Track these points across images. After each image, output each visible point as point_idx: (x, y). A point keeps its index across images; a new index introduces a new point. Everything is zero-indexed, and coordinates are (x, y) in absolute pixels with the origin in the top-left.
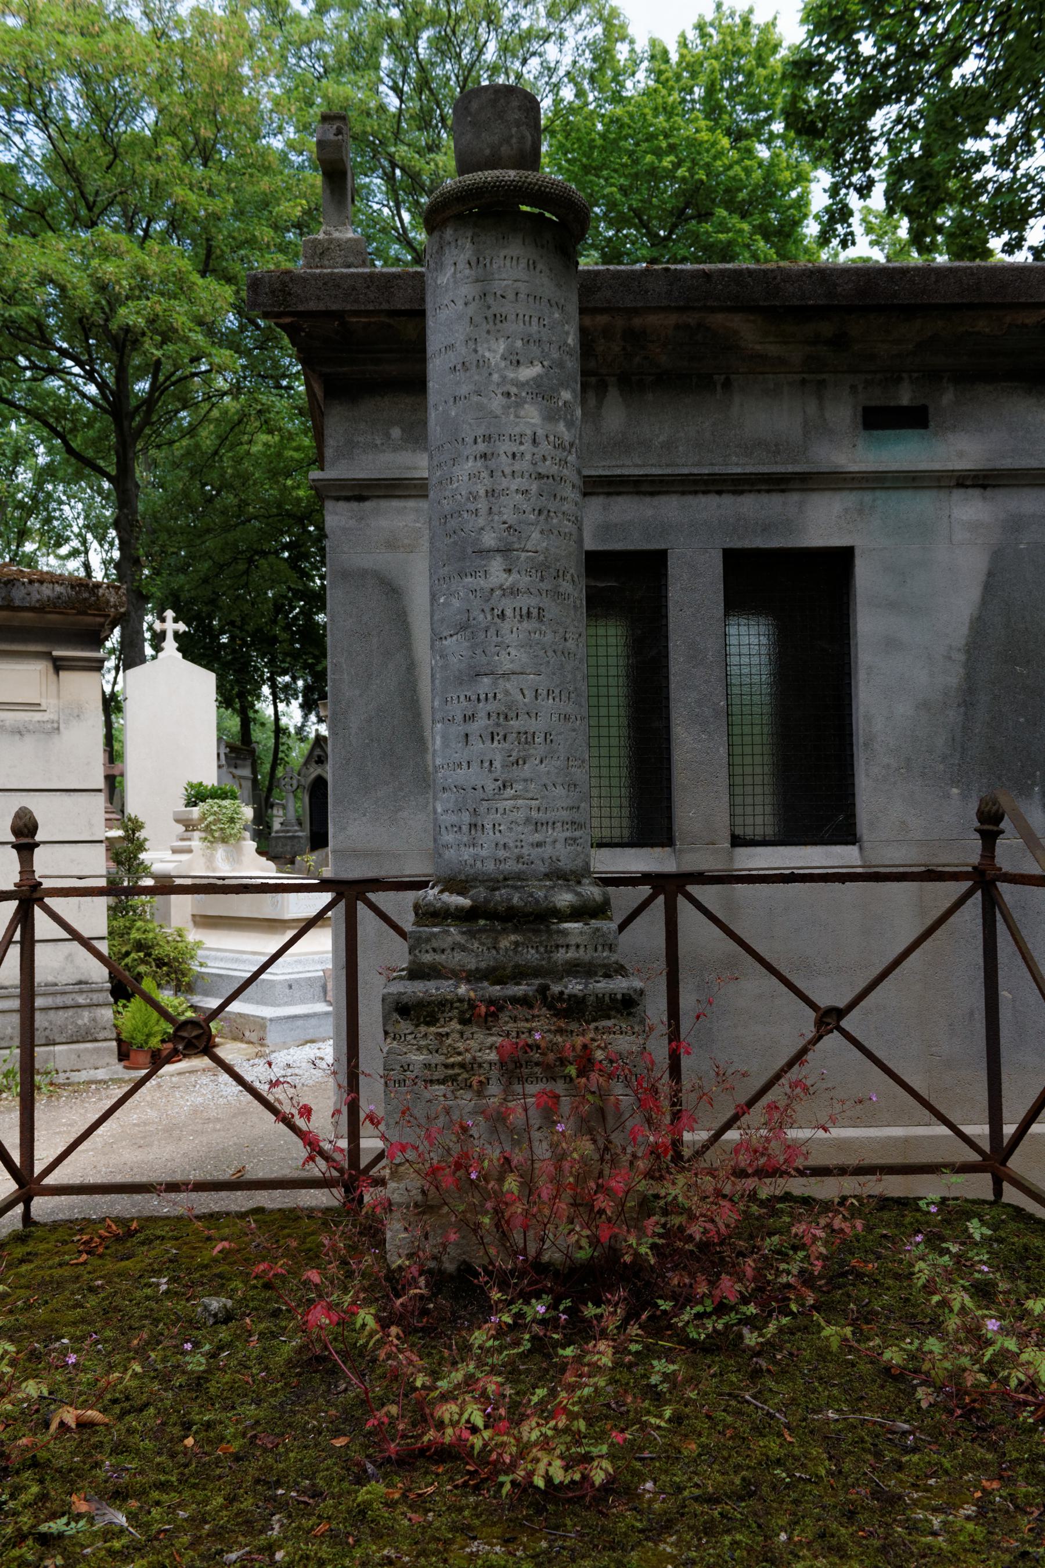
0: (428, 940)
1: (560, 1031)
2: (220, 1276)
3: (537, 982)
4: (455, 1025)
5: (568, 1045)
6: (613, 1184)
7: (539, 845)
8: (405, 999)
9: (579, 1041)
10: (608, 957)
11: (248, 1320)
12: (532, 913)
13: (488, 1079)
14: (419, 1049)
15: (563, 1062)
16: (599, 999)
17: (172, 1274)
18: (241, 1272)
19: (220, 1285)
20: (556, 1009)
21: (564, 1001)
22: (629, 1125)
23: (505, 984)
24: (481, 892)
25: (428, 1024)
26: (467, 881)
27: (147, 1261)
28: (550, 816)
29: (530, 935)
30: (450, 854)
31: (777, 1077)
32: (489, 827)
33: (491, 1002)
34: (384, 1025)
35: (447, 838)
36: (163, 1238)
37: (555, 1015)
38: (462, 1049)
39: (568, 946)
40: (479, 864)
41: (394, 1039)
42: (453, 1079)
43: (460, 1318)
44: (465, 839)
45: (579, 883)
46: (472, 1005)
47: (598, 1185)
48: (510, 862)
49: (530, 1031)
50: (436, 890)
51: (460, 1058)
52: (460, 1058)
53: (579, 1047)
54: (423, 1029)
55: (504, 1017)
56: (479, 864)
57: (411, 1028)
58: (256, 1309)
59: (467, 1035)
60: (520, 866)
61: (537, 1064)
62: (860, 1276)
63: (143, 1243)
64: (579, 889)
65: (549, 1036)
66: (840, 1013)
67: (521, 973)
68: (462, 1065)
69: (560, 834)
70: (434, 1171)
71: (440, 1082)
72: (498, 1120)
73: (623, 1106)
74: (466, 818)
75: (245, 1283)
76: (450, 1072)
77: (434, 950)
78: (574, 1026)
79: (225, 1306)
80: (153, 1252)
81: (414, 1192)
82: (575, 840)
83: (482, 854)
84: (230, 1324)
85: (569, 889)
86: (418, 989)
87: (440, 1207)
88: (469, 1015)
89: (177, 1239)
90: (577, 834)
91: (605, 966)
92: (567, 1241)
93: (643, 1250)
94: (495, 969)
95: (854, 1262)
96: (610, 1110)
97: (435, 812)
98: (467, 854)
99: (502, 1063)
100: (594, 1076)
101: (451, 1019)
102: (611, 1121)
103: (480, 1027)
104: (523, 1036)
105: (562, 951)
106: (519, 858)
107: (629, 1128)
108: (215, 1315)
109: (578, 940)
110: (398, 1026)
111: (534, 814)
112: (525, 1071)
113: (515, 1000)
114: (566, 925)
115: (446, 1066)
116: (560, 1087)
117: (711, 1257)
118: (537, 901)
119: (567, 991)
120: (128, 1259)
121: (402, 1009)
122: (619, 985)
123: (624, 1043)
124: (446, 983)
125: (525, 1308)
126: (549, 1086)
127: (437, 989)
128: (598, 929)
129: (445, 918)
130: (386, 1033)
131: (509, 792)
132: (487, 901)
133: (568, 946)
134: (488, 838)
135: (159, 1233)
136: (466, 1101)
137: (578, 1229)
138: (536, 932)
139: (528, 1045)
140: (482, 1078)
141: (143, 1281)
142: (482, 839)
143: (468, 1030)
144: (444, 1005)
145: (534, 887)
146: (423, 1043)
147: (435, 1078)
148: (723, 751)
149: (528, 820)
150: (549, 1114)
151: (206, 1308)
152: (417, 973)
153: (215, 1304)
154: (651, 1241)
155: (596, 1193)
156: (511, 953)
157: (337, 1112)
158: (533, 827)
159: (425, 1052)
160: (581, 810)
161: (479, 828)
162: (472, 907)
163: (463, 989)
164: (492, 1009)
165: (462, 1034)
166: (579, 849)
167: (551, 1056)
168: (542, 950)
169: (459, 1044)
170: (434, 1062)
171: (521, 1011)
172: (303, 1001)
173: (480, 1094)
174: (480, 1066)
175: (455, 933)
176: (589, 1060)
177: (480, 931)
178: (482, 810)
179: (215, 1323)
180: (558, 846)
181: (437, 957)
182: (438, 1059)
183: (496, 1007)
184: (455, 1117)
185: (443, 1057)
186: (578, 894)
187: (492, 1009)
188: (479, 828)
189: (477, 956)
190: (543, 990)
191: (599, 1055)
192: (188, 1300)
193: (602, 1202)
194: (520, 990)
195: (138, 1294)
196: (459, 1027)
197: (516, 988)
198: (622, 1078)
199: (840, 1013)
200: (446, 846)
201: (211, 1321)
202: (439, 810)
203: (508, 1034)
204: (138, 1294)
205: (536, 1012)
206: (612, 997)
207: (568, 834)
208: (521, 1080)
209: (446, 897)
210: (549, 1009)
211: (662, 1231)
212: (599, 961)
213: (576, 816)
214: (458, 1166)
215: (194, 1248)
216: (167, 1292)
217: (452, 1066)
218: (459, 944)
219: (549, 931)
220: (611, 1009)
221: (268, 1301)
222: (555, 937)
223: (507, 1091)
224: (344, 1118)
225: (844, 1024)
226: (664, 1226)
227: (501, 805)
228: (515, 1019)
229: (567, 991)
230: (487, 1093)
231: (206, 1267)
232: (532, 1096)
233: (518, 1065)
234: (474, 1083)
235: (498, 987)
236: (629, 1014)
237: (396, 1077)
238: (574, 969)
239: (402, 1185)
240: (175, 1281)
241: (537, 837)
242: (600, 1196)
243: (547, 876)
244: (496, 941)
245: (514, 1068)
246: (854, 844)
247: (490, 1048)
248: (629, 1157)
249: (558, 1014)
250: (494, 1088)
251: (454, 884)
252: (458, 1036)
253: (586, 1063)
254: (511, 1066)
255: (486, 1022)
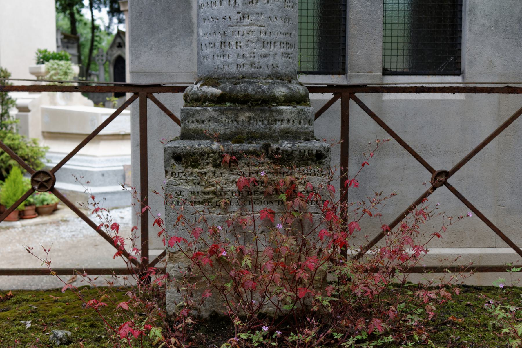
0: (194, 115)
1: (277, 172)
2: (64, 320)
3: (262, 142)
4: (210, 168)
5: (281, 181)
6: (308, 263)
7: (265, 56)
8: (179, 151)
9: (288, 179)
10: (308, 128)
11: (81, 343)
12: (260, 99)
13: (231, 202)
14: (187, 182)
15: (277, 191)
16: (302, 153)
17: (34, 319)
18: (76, 319)
19: (64, 324)
20: (274, 159)
21: (280, 154)
22: (318, 231)
23: (242, 143)
24: (228, 86)
25: (193, 167)
26: (218, 79)
27: (18, 312)
28: (273, 38)
29: (258, 113)
30: (208, 62)
31: (410, 209)
32: (233, 43)
33: (233, 154)
34: (165, 167)
35: (206, 51)
36: (28, 300)
37: (273, 163)
38: (214, 183)
39: (282, 120)
40: (226, 68)
41: (172, 175)
42: (209, 201)
43: (211, 343)
44: (218, 52)
45: (290, 82)
46: (221, 155)
47: (298, 265)
48: (246, 67)
49: (258, 172)
50: (199, 85)
51: (213, 188)
52: (213, 188)
53: (288, 182)
54: (190, 170)
55: (241, 163)
56: (226, 68)
57: (183, 169)
58: (86, 338)
59: (218, 174)
60: (253, 69)
61: (261, 193)
62: (454, 324)
63: (15, 303)
64: (290, 86)
65: (270, 176)
66: (448, 174)
67: (252, 137)
68: (214, 193)
69: (279, 50)
70: (197, 255)
71: (200, 203)
72: (236, 228)
73: (314, 219)
74: (218, 38)
75: (79, 324)
76: (207, 197)
77: (197, 121)
78: (286, 169)
79: (67, 335)
80: (22, 308)
81: (184, 269)
82: (288, 54)
83: (230, 61)
84: (70, 345)
85: (284, 85)
86: (187, 145)
87: (200, 278)
88: (219, 161)
89: (36, 301)
90: (290, 51)
91: (305, 133)
92: (279, 299)
93: (325, 303)
94: (236, 134)
95: (450, 318)
96: (306, 222)
97: (198, 35)
98: (219, 61)
99: (240, 192)
100: (297, 200)
101: (208, 164)
102: (306, 229)
103: (226, 169)
104: (253, 175)
105: (279, 123)
106: (252, 64)
107: (318, 233)
108: (61, 340)
109: (289, 117)
110: (174, 168)
111: (263, 36)
112: (254, 197)
113: (248, 152)
114: (282, 107)
115: (204, 193)
116: (275, 207)
117: (365, 310)
118: (263, 91)
119: (281, 148)
120: (6, 310)
121: (177, 157)
122: (314, 145)
123: (316, 181)
124: (205, 142)
125: (252, 335)
126: (269, 207)
127: (199, 145)
128: (302, 110)
129: (204, 102)
130: (167, 172)
131: (247, 21)
132: (231, 91)
133: (282, 120)
134: (232, 51)
135: (25, 298)
136: (217, 215)
137: (285, 291)
138: (262, 111)
139: (256, 181)
140: (227, 201)
141: (16, 322)
142: (228, 51)
143: (218, 171)
144: (203, 155)
145: (262, 83)
146: (190, 178)
147: (197, 200)
148: (380, 13)
149: (258, 40)
150: (269, 223)
151: (55, 335)
152: (185, 136)
153: (60, 333)
154: (329, 299)
155: (297, 269)
156: (246, 124)
157: (134, 228)
158: (261, 45)
159: (191, 184)
160: (292, 35)
161: (227, 44)
162: (222, 94)
163: (215, 145)
164: (234, 158)
165: (214, 173)
166: (291, 60)
167: (270, 189)
168: (266, 122)
169: (213, 180)
170: (196, 190)
171: (252, 159)
172: (111, 184)
173: (225, 210)
174: (226, 193)
175: (211, 110)
176: (294, 191)
177: (226, 110)
178: (229, 32)
179: (61, 344)
180: (277, 57)
181: (199, 126)
182: (200, 188)
183: (236, 157)
184: (210, 224)
185: (202, 188)
186: (289, 88)
187: (234, 158)
188: (227, 44)
189: (225, 125)
190: (266, 147)
191: (301, 188)
192: (44, 332)
193: (301, 274)
194: (252, 146)
195: (13, 329)
196: (212, 169)
197: (249, 145)
198: (314, 202)
199: (448, 174)
200: (206, 57)
201: (58, 343)
202: (201, 34)
203: (244, 174)
204: (13, 329)
205: (262, 159)
206: (310, 152)
207: (284, 50)
208: (251, 202)
209: (205, 88)
210: (270, 159)
211: (336, 293)
212: (302, 130)
213: (289, 39)
214: (212, 252)
215: (47, 306)
216: (30, 328)
217: (208, 193)
218: (213, 117)
219: (270, 111)
220: (308, 159)
221: (93, 333)
222: (274, 114)
223: (242, 209)
224: (139, 233)
225: (449, 181)
226: (338, 290)
227: (241, 29)
228: (248, 165)
229: (281, 148)
230: (229, 210)
231: (54, 316)
232: (258, 212)
233: (250, 193)
234: (222, 204)
235: (238, 145)
236: (320, 163)
237: (172, 198)
238: (286, 135)
239: (176, 265)
240: (36, 323)
241: (264, 51)
242: (301, 271)
243: (270, 76)
244: (237, 116)
245: (247, 195)
246: (459, 75)
247: (232, 182)
248: (317, 250)
249: (276, 161)
250: (234, 207)
251: (209, 80)
252: (212, 174)
253: (292, 193)
254: (245, 194)
255: (230, 166)
